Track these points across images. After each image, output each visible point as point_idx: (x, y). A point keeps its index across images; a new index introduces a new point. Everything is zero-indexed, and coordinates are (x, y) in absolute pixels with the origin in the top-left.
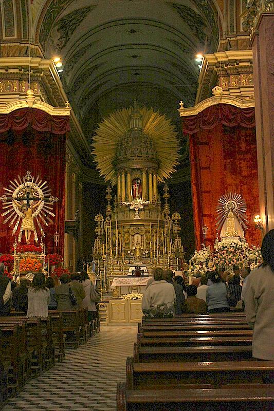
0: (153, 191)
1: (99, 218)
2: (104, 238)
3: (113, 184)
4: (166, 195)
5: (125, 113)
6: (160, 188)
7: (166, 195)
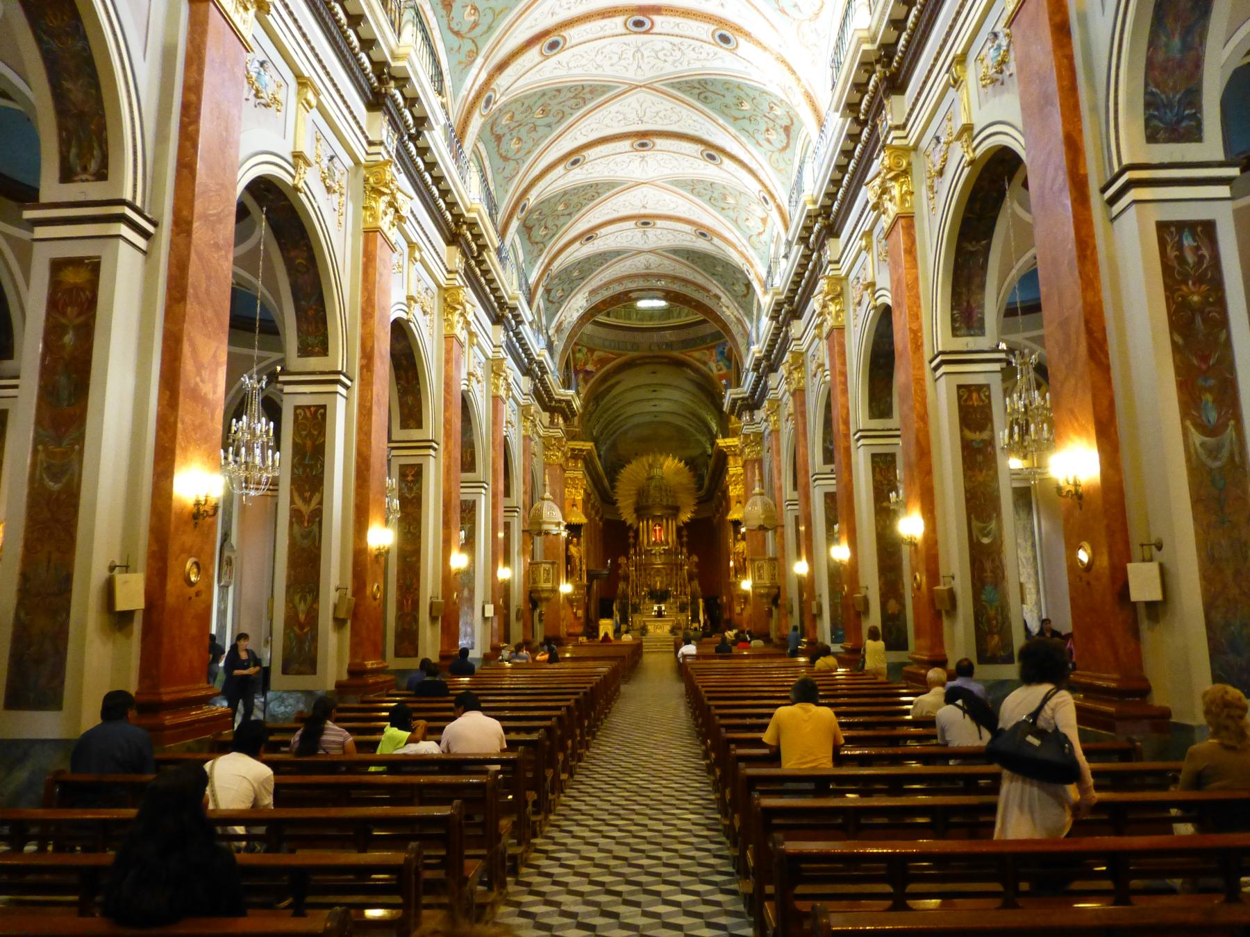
0: (672, 538)
1: (622, 560)
2: (626, 578)
3: (635, 527)
4: (685, 539)
5: (647, 460)
6: (679, 530)
7: (685, 539)
